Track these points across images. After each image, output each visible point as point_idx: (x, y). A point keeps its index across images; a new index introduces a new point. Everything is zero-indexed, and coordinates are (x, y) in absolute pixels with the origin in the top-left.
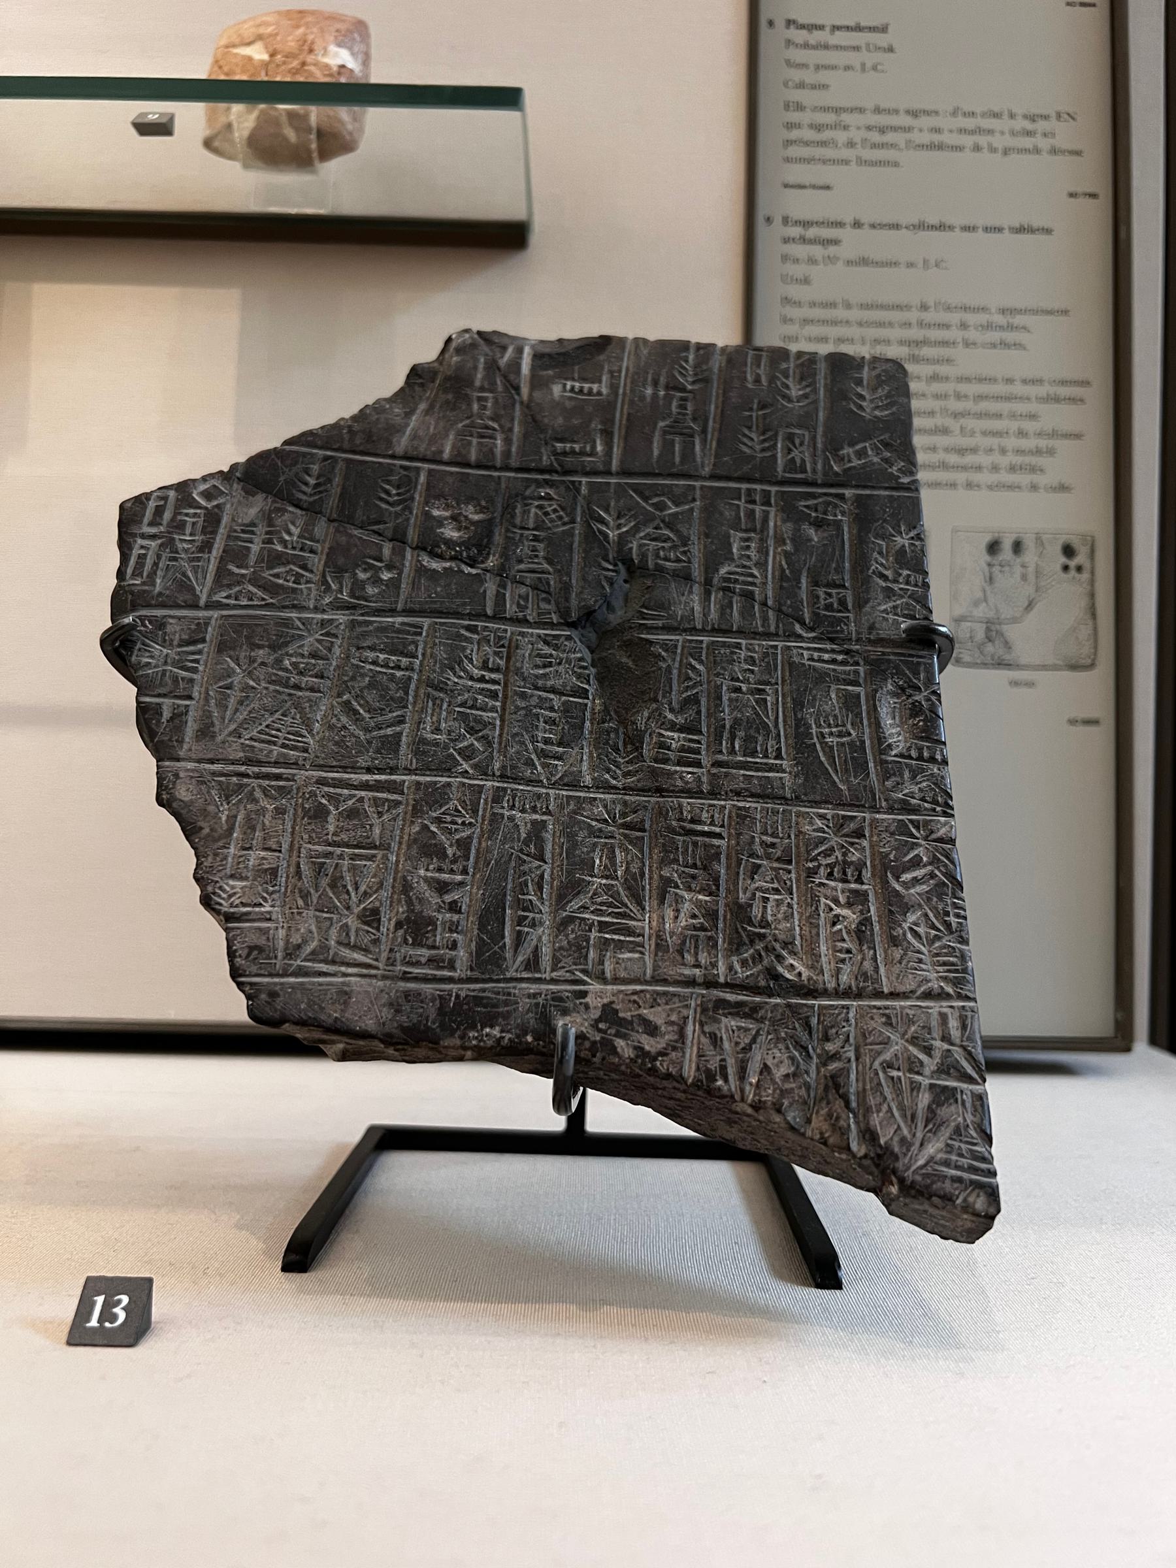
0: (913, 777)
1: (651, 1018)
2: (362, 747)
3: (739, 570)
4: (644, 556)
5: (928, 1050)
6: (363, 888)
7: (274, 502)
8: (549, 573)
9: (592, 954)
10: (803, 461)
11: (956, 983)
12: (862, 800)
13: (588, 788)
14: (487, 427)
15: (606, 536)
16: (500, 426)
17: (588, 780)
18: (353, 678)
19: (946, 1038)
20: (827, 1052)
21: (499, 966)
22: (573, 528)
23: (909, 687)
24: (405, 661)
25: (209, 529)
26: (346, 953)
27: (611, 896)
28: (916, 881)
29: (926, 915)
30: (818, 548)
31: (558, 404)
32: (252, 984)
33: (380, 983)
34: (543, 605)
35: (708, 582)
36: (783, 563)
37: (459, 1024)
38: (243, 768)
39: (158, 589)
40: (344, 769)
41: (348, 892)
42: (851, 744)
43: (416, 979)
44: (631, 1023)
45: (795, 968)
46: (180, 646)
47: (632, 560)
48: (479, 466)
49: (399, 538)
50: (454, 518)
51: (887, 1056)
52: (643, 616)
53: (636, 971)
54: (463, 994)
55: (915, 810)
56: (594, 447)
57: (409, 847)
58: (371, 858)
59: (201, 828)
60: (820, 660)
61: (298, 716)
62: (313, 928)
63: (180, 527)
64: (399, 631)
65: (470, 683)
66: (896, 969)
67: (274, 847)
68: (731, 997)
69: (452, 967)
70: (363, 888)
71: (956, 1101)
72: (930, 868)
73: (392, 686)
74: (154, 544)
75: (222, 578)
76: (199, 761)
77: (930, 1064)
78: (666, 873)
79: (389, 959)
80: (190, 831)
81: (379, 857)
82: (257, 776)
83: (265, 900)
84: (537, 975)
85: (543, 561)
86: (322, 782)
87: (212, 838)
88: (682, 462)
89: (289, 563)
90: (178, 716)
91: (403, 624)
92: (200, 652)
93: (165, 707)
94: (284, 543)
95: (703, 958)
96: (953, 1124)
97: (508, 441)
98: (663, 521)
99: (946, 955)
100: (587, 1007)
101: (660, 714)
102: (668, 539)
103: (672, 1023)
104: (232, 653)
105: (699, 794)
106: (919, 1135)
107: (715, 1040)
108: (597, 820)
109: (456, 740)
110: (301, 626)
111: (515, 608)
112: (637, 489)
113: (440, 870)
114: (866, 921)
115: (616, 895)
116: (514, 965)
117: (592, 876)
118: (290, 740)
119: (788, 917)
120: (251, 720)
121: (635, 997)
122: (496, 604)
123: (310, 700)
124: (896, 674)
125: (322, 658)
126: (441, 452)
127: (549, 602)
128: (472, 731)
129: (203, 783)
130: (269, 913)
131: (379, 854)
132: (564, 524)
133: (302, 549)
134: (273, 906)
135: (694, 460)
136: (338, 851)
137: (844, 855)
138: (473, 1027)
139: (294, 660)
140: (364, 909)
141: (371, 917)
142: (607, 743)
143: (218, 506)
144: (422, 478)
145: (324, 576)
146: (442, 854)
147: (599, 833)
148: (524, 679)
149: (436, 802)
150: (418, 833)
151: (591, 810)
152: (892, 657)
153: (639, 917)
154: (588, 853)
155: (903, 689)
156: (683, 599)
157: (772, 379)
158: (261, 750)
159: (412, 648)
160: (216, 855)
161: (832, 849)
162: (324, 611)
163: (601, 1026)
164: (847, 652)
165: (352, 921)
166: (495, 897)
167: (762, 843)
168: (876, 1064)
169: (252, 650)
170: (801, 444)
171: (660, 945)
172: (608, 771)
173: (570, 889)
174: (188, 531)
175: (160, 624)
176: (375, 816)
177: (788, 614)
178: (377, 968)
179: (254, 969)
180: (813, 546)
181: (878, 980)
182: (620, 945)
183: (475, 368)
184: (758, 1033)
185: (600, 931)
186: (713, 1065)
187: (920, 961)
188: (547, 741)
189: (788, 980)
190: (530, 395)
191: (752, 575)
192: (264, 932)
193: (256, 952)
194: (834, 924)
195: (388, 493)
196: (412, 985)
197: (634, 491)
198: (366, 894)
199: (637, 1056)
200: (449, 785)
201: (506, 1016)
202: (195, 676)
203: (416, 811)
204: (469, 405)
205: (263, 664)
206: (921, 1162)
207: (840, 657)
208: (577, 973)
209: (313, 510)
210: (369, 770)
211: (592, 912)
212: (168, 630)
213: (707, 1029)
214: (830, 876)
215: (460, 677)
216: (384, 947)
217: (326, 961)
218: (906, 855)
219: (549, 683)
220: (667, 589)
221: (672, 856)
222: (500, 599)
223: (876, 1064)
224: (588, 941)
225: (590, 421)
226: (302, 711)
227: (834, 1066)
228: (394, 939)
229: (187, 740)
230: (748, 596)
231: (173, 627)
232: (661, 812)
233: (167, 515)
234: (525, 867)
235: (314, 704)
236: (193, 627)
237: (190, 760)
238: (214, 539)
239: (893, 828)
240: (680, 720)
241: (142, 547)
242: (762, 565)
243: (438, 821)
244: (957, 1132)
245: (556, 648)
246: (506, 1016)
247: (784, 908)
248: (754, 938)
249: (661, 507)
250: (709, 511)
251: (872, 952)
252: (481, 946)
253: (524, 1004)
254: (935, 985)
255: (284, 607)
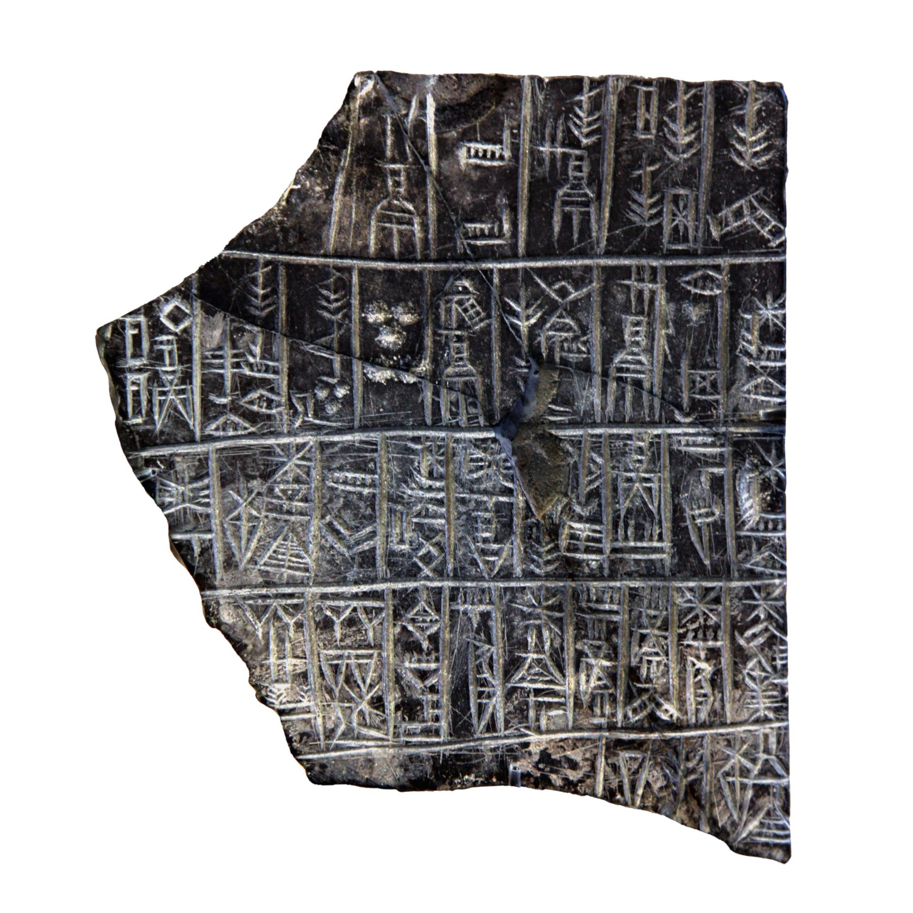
0: (759, 549)
1: (573, 757)
2: (348, 563)
3: (629, 358)
4: (551, 350)
5: (754, 761)
6: (368, 681)
7: (232, 321)
8: (473, 376)
9: (532, 714)
10: (686, 228)
11: (776, 710)
12: (722, 570)
13: (519, 578)
14: (404, 211)
15: (517, 330)
16: (415, 208)
17: (518, 571)
18: (331, 500)
19: (767, 751)
20: (688, 769)
21: (469, 731)
22: (489, 325)
23: (762, 464)
24: (368, 478)
25: (185, 358)
26: (364, 731)
27: (542, 668)
28: (754, 636)
29: (760, 662)
30: (695, 330)
31: (465, 175)
32: (308, 760)
33: (391, 751)
34: (472, 410)
35: (605, 374)
36: (666, 347)
37: (447, 775)
38: (264, 591)
39: (159, 426)
40: (338, 583)
41: (358, 686)
42: (715, 524)
43: (415, 745)
44: (560, 762)
45: (669, 710)
46: (190, 483)
47: (541, 354)
48: (402, 260)
49: (345, 348)
50: (388, 322)
51: (727, 768)
52: (553, 413)
53: (561, 723)
54: (447, 754)
55: (760, 576)
56: (501, 228)
57: (395, 645)
58: (370, 656)
59: (246, 646)
60: (695, 444)
61: (295, 539)
62: (340, 716)
63: (158, 357)
64: (359, 450)
65: (421, 493)
66: (736, 706)
67: (301, 655)
68: (625, 736)
69: (437, 733)
70: (368, 681)
71: (769, 794)
72: (765, 624)
73: (362, 504)
74: (142, 377)
75: (209, 411)
76: (231, 588)
77: (756, 769)
78: (579, 646)
79: (394, 733)
80: (239, 648)
81: (376, 655)
82: (277, 596)
83: (303, 697)
84: (495, 734)
85: (467, 363)
86: (324, 597)
87: (255, 653)
88: (580, 240)
89: (258, 387)
90: (206, 549)
91: (362, 442)
92: (207, 487)
93: (194, 542)
94: (251, 366)
95: (607, 710)
96: (766, 809)
97: (425, 226)
98: (565, 310)
99: (771, 690)
100: (530, 754)
101: (570, 509)
102: (570, 329)
103: (586, 760)
104: (232, 486)
105: (602, 578)
106: (744, 818)
107: (615, 768)
108: (528, 606)
109: (417, 549)
110: (281, 453)
111: (449, 416)
112: (541, 272)
113: (419, 661)
114: (718, 672)
115: (545, 667)
116: (480, 726)
117: (526, 653)
118: (293, 562)
119: (666, 673)
120: (262, 548)
121: (562, 744)
122: (434, 414)
123: (302, 525)
124: (753, 454)
125: (303, 483)
126: (366, 247)
127: (475, 406)
128: (428, 538)
129: (238, 607)
130: (308, 707)
131: (375, 652)
132: (481, 320)
133: (266, 371)
134: (309, 701)
135: (590, 237)
136: (346, 652)
137: (705, 620)
138: (457, 776)
139: (282, 487)
140: (372, 698)
141: (378, 703)
142: (530, 538)
143: (185, 331)
144: (355, 279)
145: (290, 399)
146: (420, 650)
147: (530, 616)
148: (463, 486)
149: (409, 606)
150: (400, 634)
151: (522, 598)
152: (750, 438)
153: (562, 682)
154: (522, 634)
155: (756, 466)
156: (585, 393)
157: (661, 124)
158: (274, 574)
159: (371, 465)
160: (262, 666)
161: (696, 617)
162: (295, 435)
163: (541, 766)
164: (715, 435)
165: (365, 706)
166: (461, 679)
167: (648, 615)
168: (720, 775)
169: (248, 481)
170: (685, 207)
171: (578, 704)
172: (533, 561)
173: (513, 665)
174: (167, 361)
175: (170, 463)
176: (367, 621)
177: (671, 402)
178: (388, 740)
179: (306, 749)
180: (691, 327)
181: (723, 715)
182: (550, 706)
183: (384, 132)
184: (643, 761)
185: (535, 696)
186: (614, 785)
187: (753, 697)
188: (485, 541)
189: (663, 720)
190: (439, 166)
191: (640, 362)
192: (307, 721)
193: (305, 738)
194: (696, 676)
195: (328, 300)
196: (412, 751)
197: (540, 276)
198: (371, 686)
199: (565, 785)
200: (416, 590)
201: (478, 766)
202: (210, 511)
203: (397, 616)
204: (384, 182)
205: (259, 494)
206: (744, 835)
207: (710, 440)
208: (522, 730)
209: (268, 324)
210: (356, 583)
211: (529, 681)
212: (177, 469)
213: (610, 761)
214: (695, 638)
215: (412, 489)
216: (391, 724)
217: (353, 739)
218: (749, 616)
219: (483, 487)
220: (571, 383)
221: (583, 633)
222: (436, 406)
223: (720, 775)
224: (527, 704)
225: (495, 196)
226: (297, 534)
227: (692, 777)
228: (396, 718)
229: (218, 571)
230: (638, 384)
231: (181, 465)
232: (576, 595)
233: (146, 345)
234: (479, 652)
235: (306, 526)
236: (197, 463)
237: (223, 587)
238: (191, 368)
239: (741, 595)
240: (585, 513)
241: (133, 383)
242: (650, 350)
243: (413, 621)
244: (768, 814)
245: (485, 450)
246: (478, 766)
247: (662, 667)
248: (642, 691)
249: (563, 293)
250: (606, 293)
251: (720, 695)
252: (455, 718)
253: (488, 756)
254: (761, 713)
255: (263, 434)
